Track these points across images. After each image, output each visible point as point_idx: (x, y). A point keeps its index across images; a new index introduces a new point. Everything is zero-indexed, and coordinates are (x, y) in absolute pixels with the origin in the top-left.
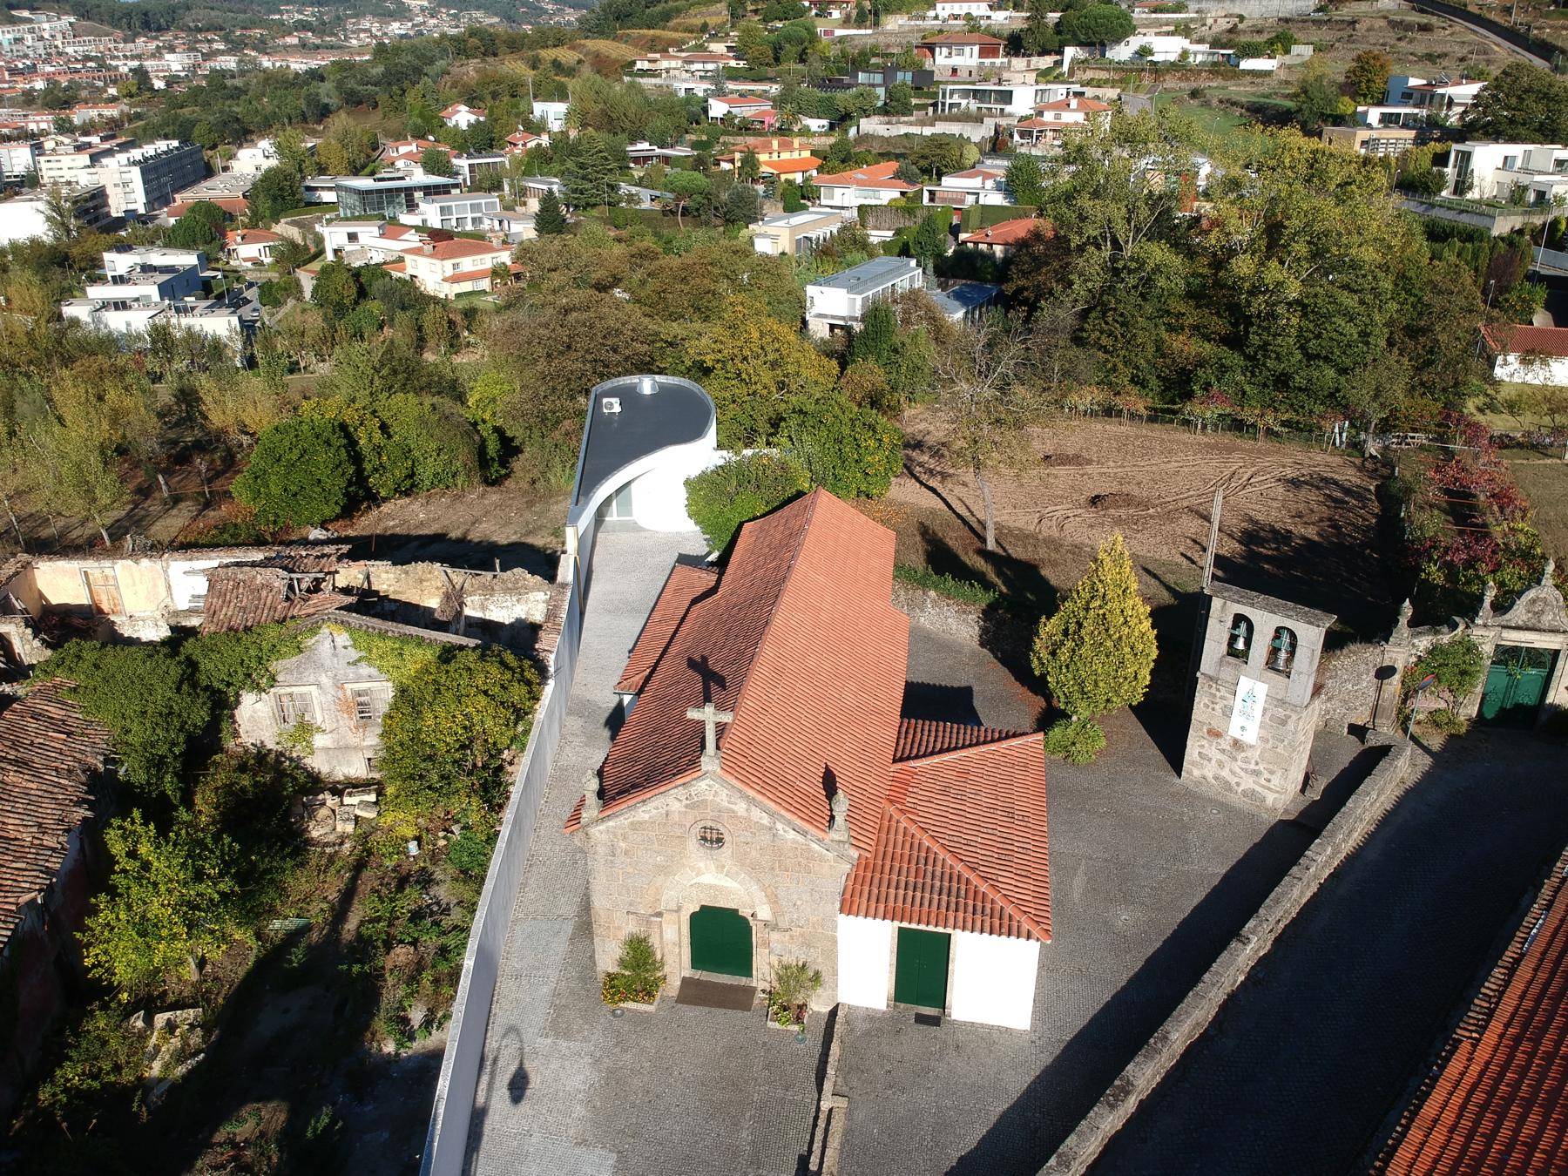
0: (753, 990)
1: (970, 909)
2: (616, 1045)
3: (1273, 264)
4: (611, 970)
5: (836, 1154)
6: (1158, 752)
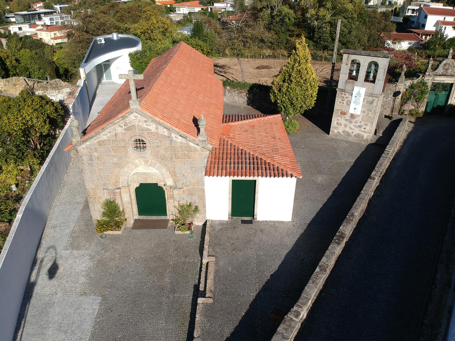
0: (168, 221)
1: (264, 168)
2: (102, 250)
3: (322, 9)
4: (99, 219)
5: (212, 282)
6: (319, 128)
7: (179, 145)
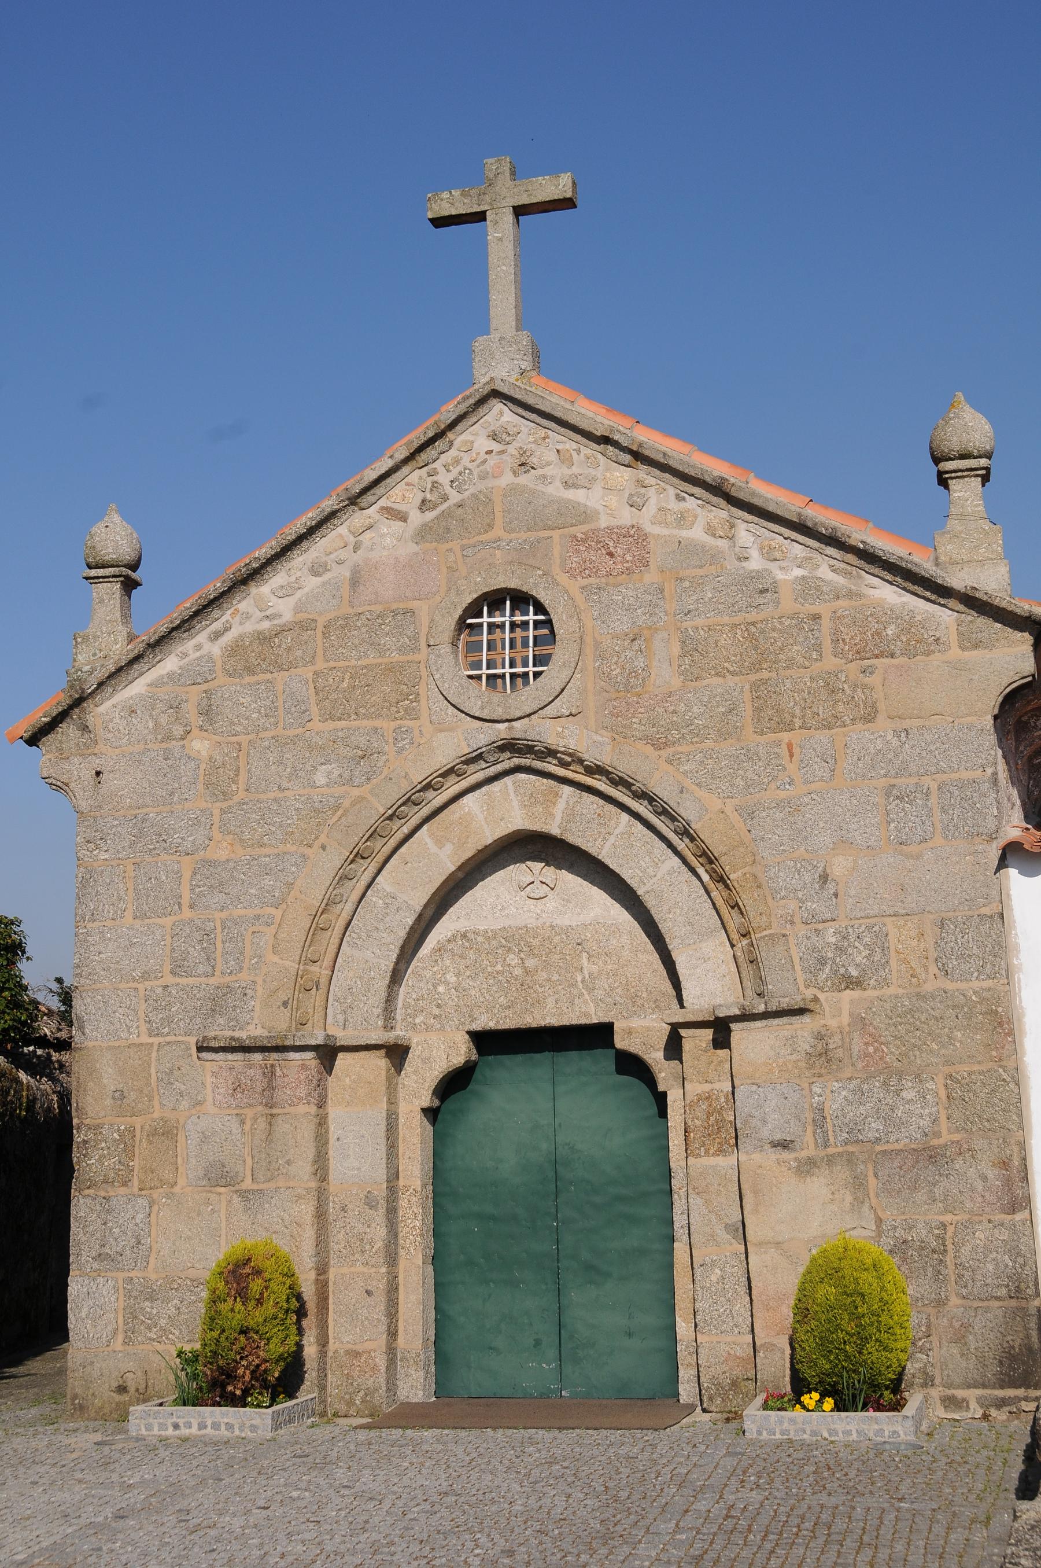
7: (788, 604)
